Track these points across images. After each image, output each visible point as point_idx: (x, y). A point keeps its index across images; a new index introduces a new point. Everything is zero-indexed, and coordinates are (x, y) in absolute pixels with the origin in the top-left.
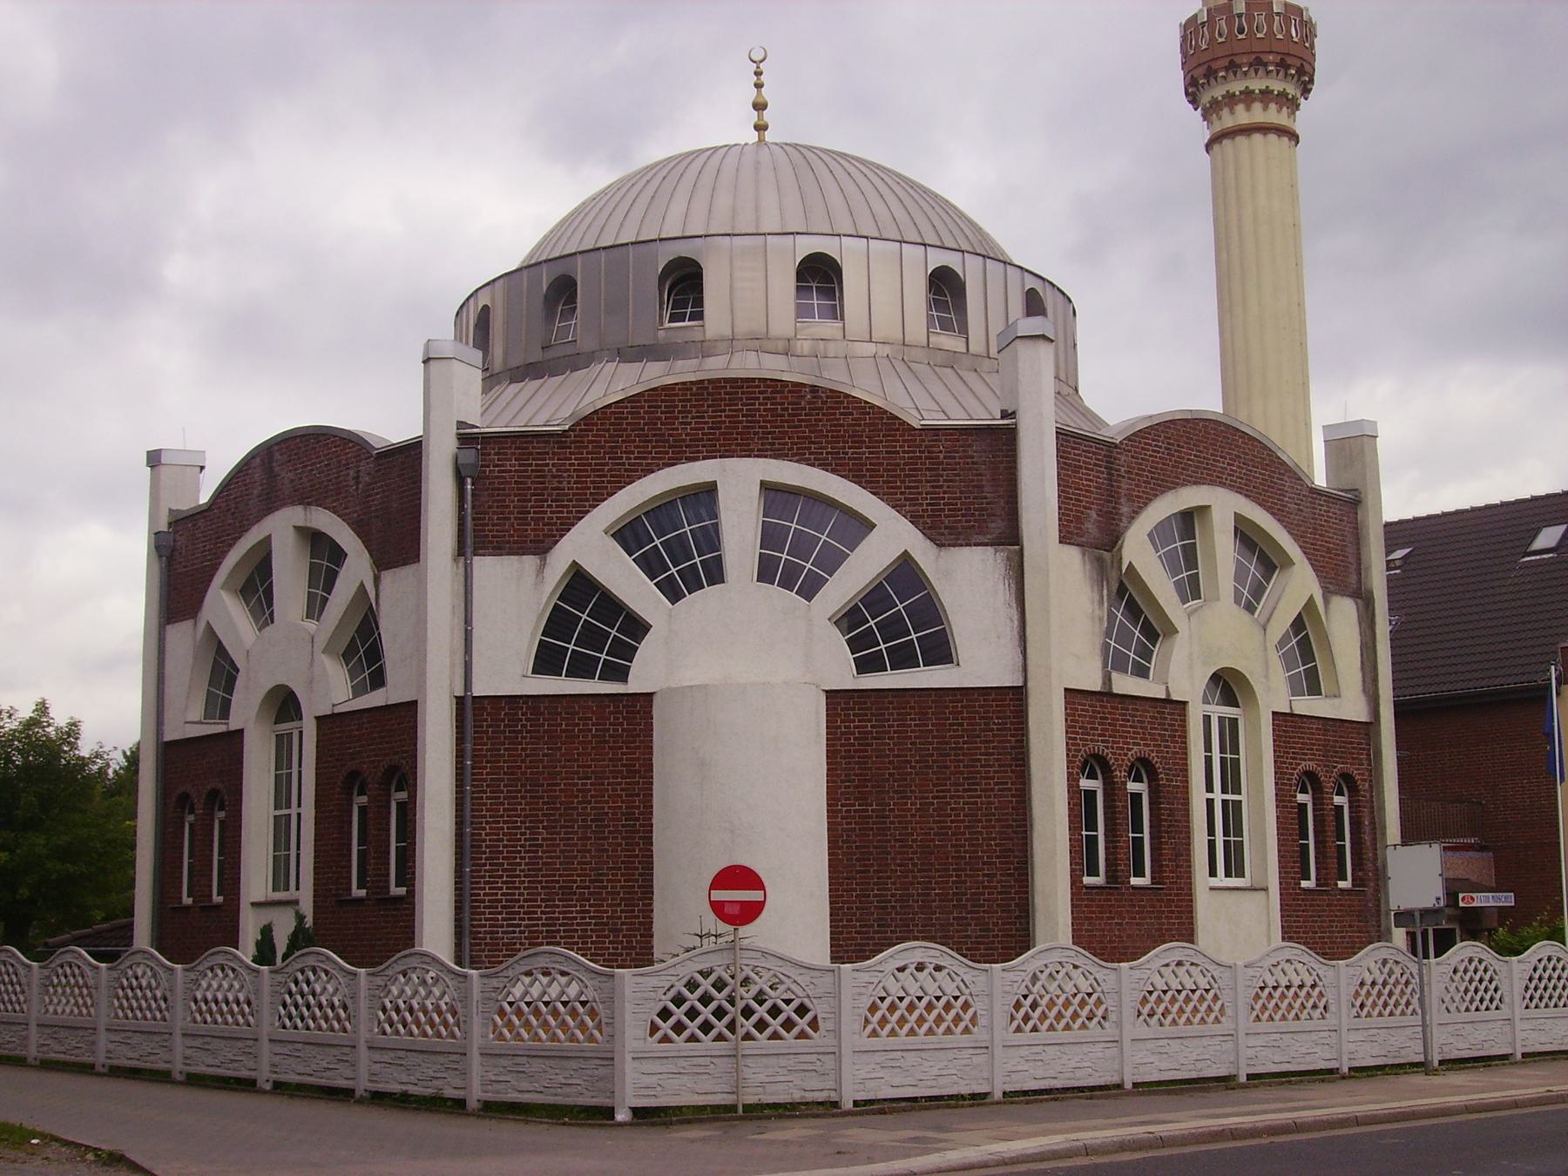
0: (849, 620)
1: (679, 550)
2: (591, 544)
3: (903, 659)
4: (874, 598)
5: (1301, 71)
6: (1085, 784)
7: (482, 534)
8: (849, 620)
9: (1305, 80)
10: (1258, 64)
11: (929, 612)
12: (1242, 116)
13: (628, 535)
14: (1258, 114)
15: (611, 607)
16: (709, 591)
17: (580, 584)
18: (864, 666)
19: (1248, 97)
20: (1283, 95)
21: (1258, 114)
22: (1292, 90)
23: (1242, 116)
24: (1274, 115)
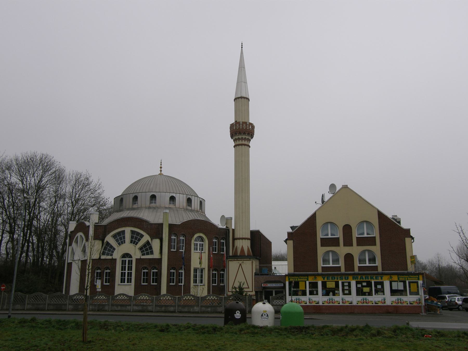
0: (141, 249)
1: (120, 238)
2: (109, 239)
3: (148, 254)
4: (144, 246)
5: (252, 135)
6: (172, 271)
7: (96, 237)
8: (141, 249)
9: (252, 135)
10: (244, 133)
11: (151, 248)
12: (240, 142)
13: (114, 236)
14: (244, 142)
15: (111, 247)
16: (124, 245)
17: (108, 243)
18: (143, 255)
19: (242, 139)
20: (248, 139)
21: (244, 142)
22: (250, 138)
23: (240, 142)
24: (246, 143)
